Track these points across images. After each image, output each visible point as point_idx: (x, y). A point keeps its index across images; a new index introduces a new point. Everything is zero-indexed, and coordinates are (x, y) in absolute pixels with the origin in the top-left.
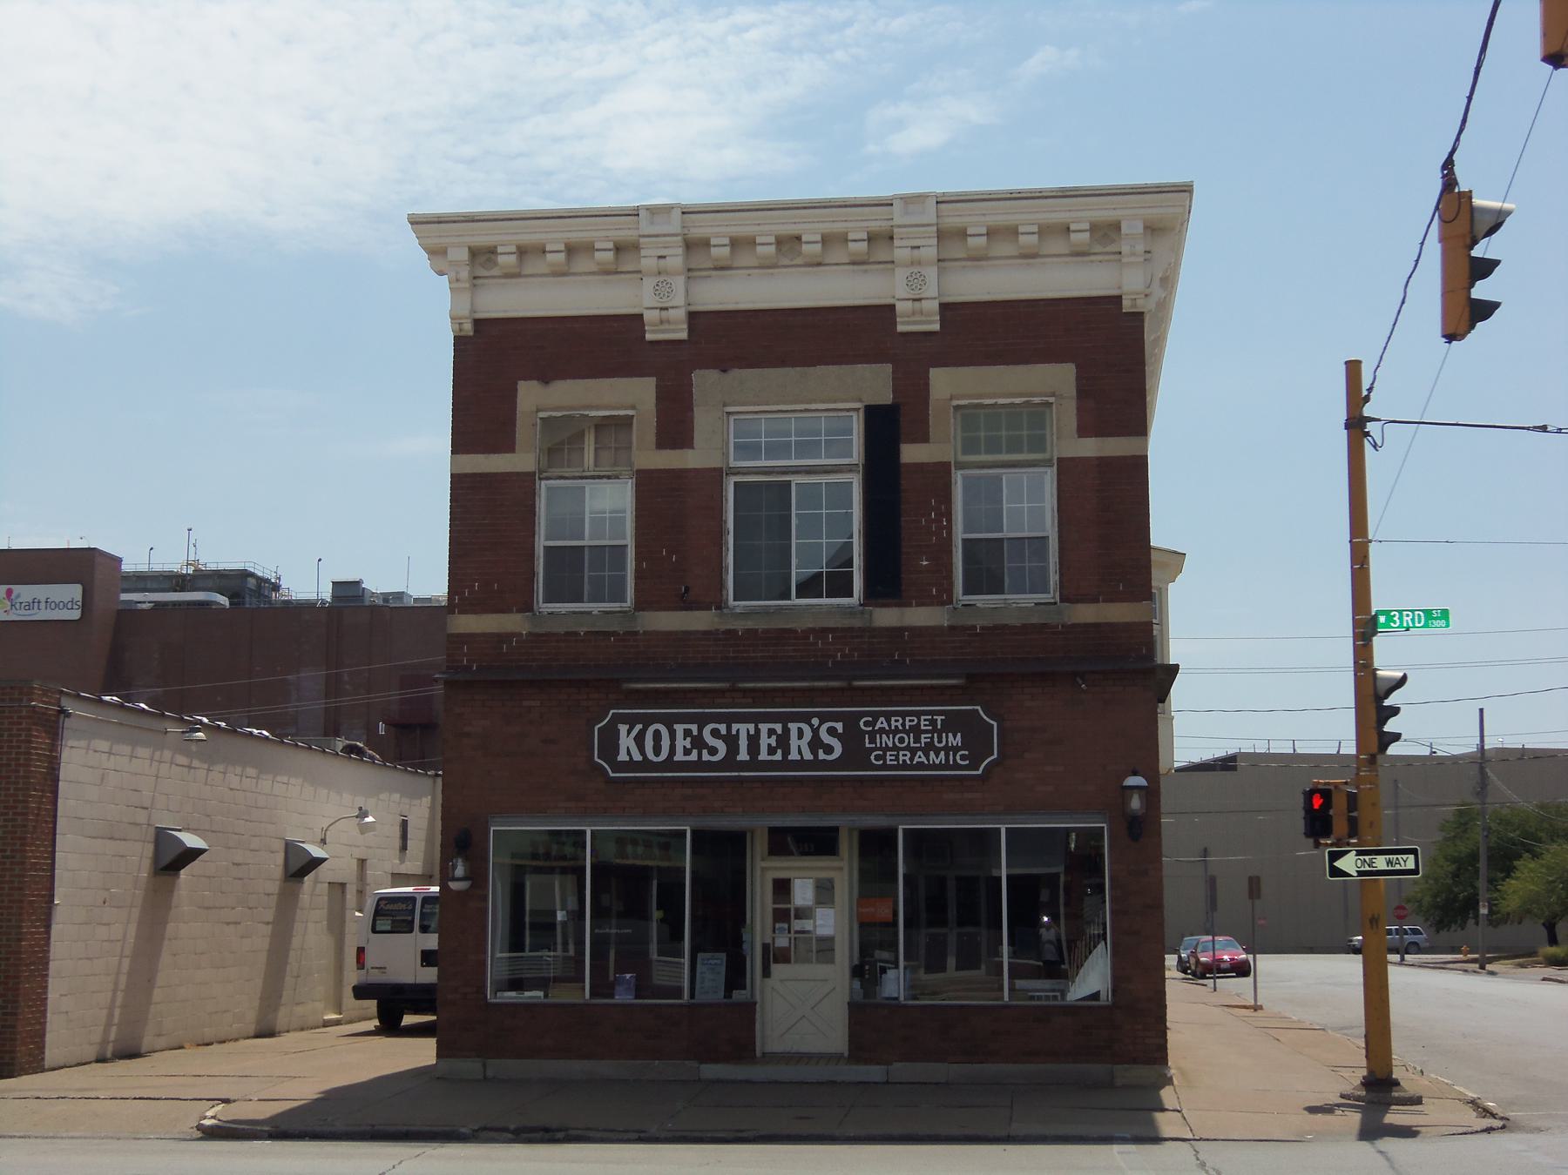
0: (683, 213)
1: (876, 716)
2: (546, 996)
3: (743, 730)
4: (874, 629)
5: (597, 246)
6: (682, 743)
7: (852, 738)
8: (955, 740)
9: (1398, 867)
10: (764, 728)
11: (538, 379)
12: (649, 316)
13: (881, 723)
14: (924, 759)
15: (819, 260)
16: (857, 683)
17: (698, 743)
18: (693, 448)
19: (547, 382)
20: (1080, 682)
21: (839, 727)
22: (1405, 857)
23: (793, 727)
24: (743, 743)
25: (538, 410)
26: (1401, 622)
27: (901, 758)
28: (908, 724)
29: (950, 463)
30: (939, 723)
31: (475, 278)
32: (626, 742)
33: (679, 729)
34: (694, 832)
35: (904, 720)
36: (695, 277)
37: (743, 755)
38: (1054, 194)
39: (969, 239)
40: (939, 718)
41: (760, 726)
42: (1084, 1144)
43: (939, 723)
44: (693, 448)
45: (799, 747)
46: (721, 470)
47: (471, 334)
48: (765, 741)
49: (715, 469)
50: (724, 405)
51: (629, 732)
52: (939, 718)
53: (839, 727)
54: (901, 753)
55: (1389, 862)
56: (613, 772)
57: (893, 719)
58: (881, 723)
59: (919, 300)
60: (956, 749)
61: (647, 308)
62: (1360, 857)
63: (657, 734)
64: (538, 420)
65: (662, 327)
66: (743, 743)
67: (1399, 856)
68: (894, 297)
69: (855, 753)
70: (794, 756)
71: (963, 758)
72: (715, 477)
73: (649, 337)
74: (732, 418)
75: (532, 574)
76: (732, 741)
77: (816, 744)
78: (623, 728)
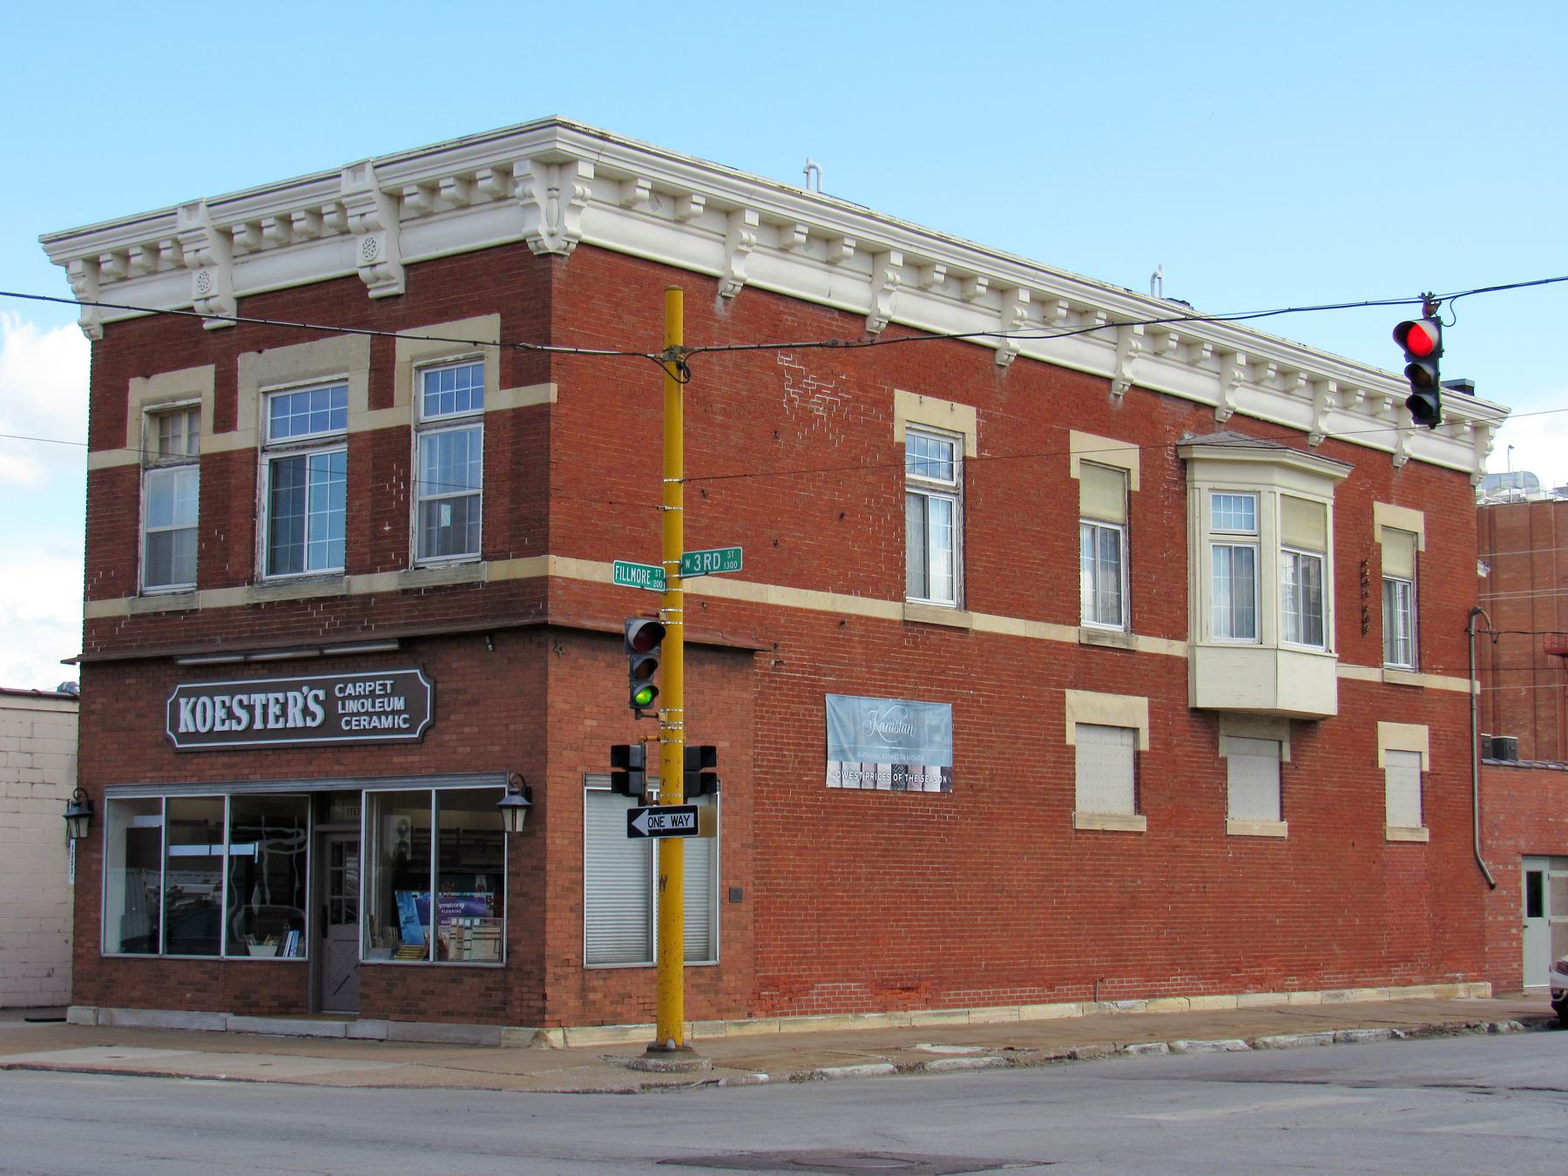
0: (376, 167)
1: (346, 681)
2: (279, 952)
3: (258, 699)
4: (352, 597)
5: (161, 246)
6: (221, 713)
7: (329, 704)
8: (399, 703)
9: (681, 826)
10: (272, 696)
11: (142, 376)
12: (364, 274)
13: (350, 690)
14: (377, 724)
15: (256, 247)
16: (328, 651)
17: (231, 714)
18: (236, 430)
19: (148, 377)
20: (488, 641)
21: (321, 694)
22: (687, 815)
23: (290, 695)
24: (258, 712)
25: (412, 361)
26: (702, 566)
27: (362, 723)
28: (368, 689)
29: (409, 427)
30: (389, 687)
31: (401, 222)
32: (185, 714)
33: (218, 699)
34: (232, 798)
35: (355, 687)
36: (406, 228)
37: (258, 725)
38: (454, 145)
39: (235, 237)
40: (389, 682)
41: (288, 694)
42: (41, 1051)
43: (389, 687)
44: (236, 430)
45: (295, 719)
46: (256, 449)
47: (101, 337)
48: (274, 710)
49: (249, 450)
50: (260, 386)
51: (188, 703)
52: (389, 682)
53: (321, 694)
54: (362, 718)
55: (674, 821)
56: (415, 733)
57: (358, 685)
58: (350, 690)
59: (373, 266)
60: (399, 712)
61: (362, 267)
62: (653, 816)
63: (204, 705)
64: (143, 414)
65: (379, 284)
66: (258, 712)
67: (682, 815)
68: (355, 266)
69: (331, 723)
70: (290, 724)
71: (405, 721)
72: (251, 456)
73: (372, 294)
74: (270, 396)
75: (136, 559)
76: (250, 709)
77: (306, 711)
78: (183, 701)
